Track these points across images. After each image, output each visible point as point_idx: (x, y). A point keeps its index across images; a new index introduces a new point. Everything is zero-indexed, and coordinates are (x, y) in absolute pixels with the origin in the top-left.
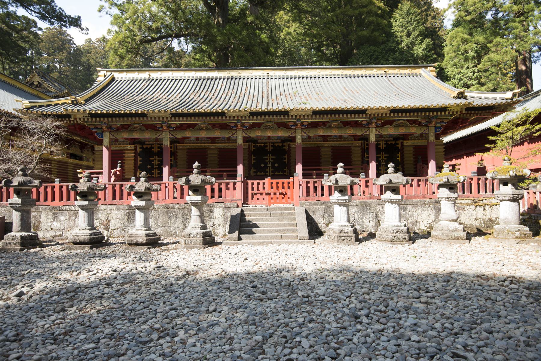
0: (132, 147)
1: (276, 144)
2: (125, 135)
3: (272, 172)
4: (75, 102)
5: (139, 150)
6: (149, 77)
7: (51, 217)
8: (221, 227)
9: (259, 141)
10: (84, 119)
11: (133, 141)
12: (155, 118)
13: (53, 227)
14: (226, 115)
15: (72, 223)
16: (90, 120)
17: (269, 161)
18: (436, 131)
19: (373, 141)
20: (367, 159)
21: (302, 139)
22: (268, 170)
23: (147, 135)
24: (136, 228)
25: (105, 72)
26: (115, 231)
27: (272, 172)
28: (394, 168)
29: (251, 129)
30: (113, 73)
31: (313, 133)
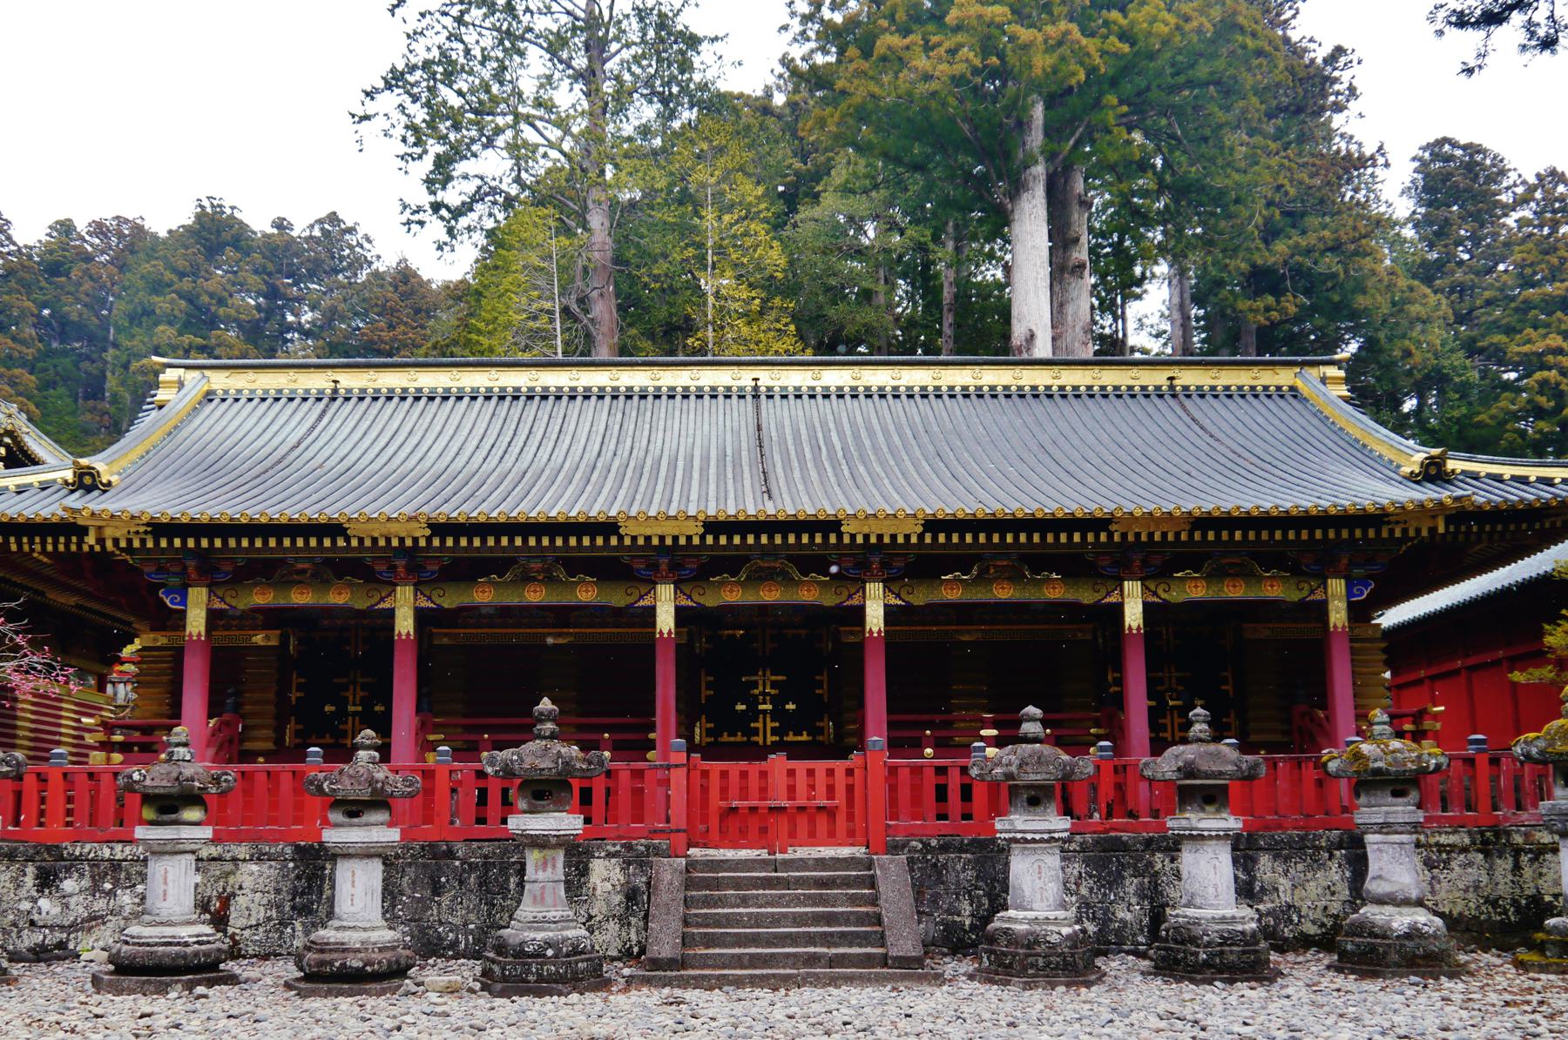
2: (261, 598)
3: (774, 731)
4: (87, 480)
6: (335, 391)
7: (29, 880)
8: (613, 926)
10: (130, 541)
12: (374, 540)
13: (36, 917)
14: (622, 531)
15: (100, 905)
16: (150, 544)
17: (764, 694)
19: (1134, 625)
20: (1114, 689)
21: (887, 614)
22: (759, 725)
24: (335, 923)
26: (247, 933)
27: (774, 731)
28: (1209, 724)
30: (207, 373)
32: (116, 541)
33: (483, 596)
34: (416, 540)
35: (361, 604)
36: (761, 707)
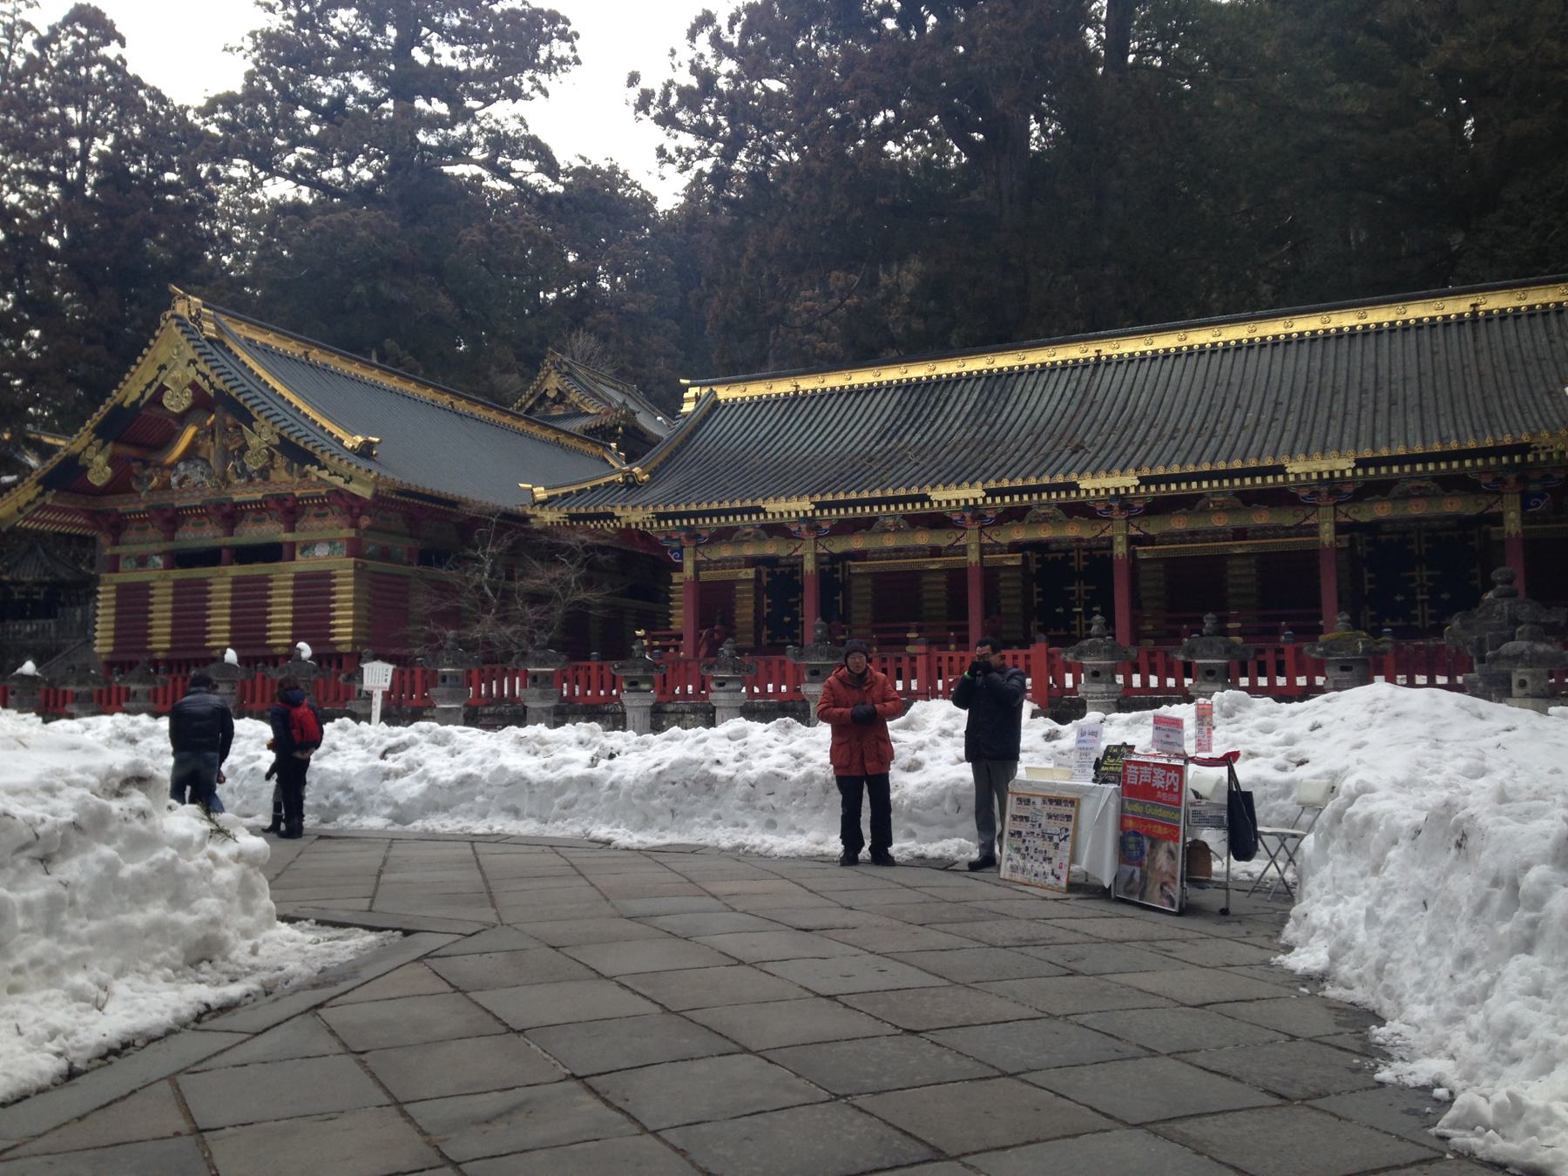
0: (750, 573)
1: (1098, 553)
2: (726, 552)
4: (631, 480)
5: (765, 579)
6: (796, 393)
9: (1054, 546)
10: (644, 524)
11: (752, 562)
12: (781, 514)
16: (655, 525)
18: (1525, 506)
23: (770, 549)
25: (697, 389)
29: (1001, 524)
30: (714, 389)
31: (1154, 527)
32: (637, 524)
33: (857, 543)
34: (805, 512)
35: (784, 552)
36: (1075, 610)
